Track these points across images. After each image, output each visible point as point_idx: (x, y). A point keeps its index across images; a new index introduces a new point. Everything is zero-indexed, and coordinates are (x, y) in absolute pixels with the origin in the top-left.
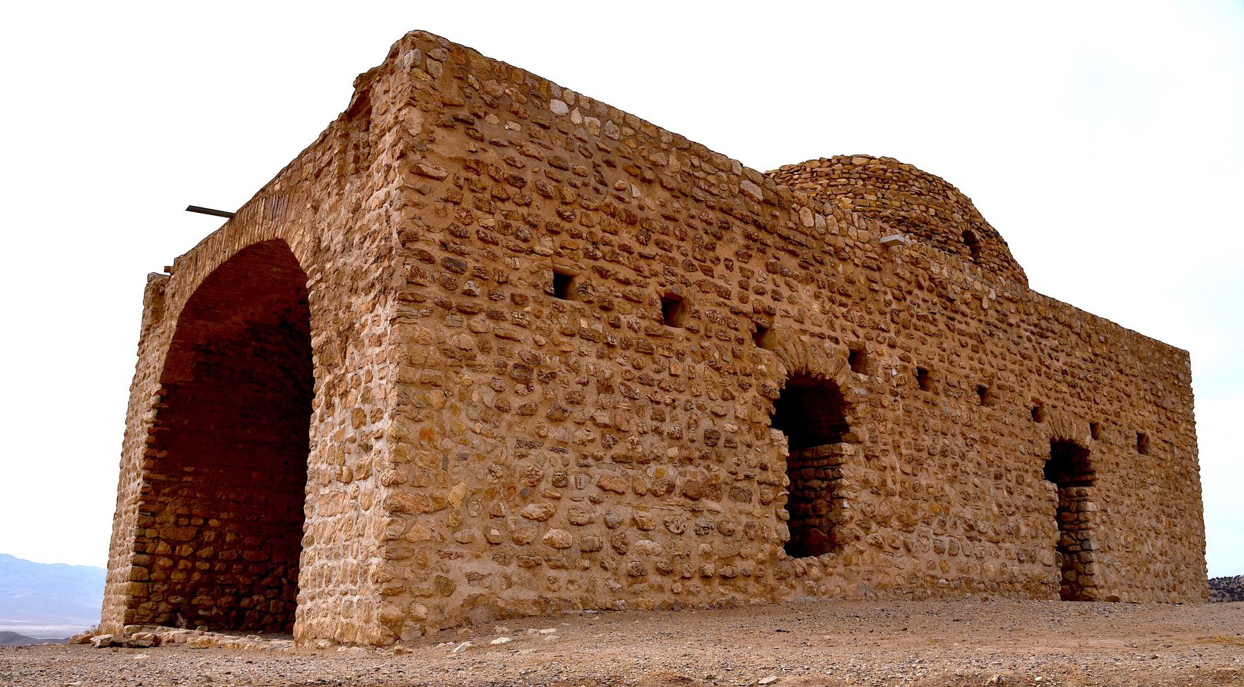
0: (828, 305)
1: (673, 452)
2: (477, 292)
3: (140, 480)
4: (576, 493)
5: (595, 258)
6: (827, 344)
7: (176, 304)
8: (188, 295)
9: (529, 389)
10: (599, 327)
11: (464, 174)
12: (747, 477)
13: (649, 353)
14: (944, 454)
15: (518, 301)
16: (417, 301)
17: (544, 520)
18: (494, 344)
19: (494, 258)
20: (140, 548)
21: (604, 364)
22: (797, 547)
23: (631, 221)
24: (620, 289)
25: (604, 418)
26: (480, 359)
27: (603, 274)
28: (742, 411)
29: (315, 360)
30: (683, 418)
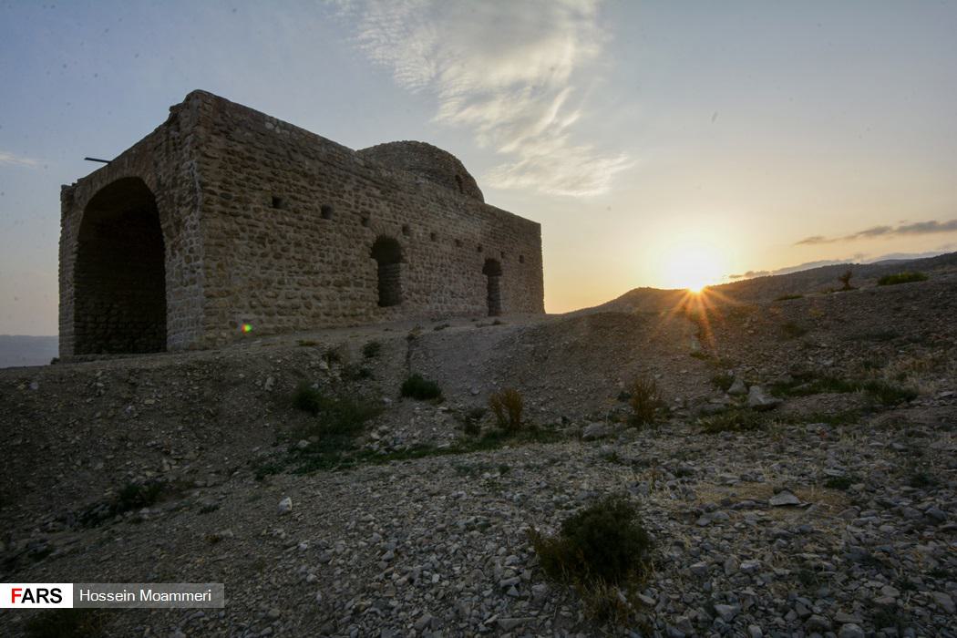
0: (393, 209)
1: (330, 268)
2: (238, 206)
3: (72, 288)
4: (288, 286)
5: (290, 191)
6: (393, 224)
7: (83, 204)
8: (88, 199)
9: (265, 246)
10: (295, 220)
11: (227, 156)
12: (361, 278)
13: (316, 230)
14: (442, 265)
15: (257, 211)
16: (210, 211)
17: (276, 297)
18: (248, 228)
19: (243, 192)
20: (77, 319)
21: (297, 235)
22: (381, 304)
23: (305, 175)
24: (302, 204)
25: (299, 256)
26: (242, 234)
27: (295, 199)
28: (358, 252)
29: (164, 234)
30: (333, 255)
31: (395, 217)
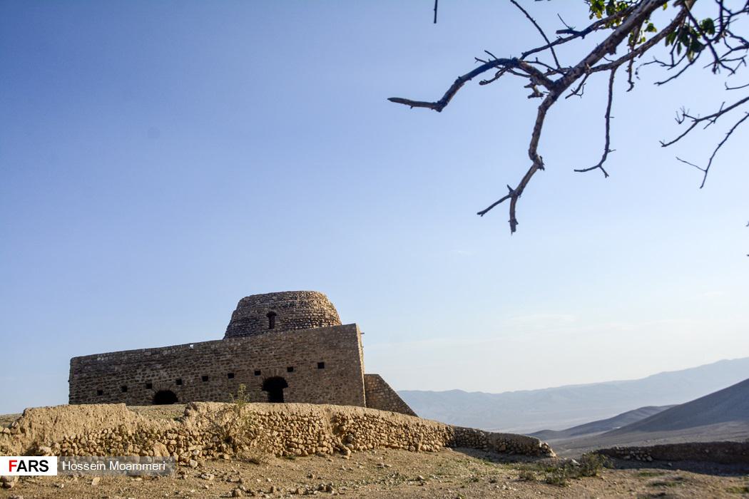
14: (212, 396)
23: (114, 375)
31: (170, 377)
